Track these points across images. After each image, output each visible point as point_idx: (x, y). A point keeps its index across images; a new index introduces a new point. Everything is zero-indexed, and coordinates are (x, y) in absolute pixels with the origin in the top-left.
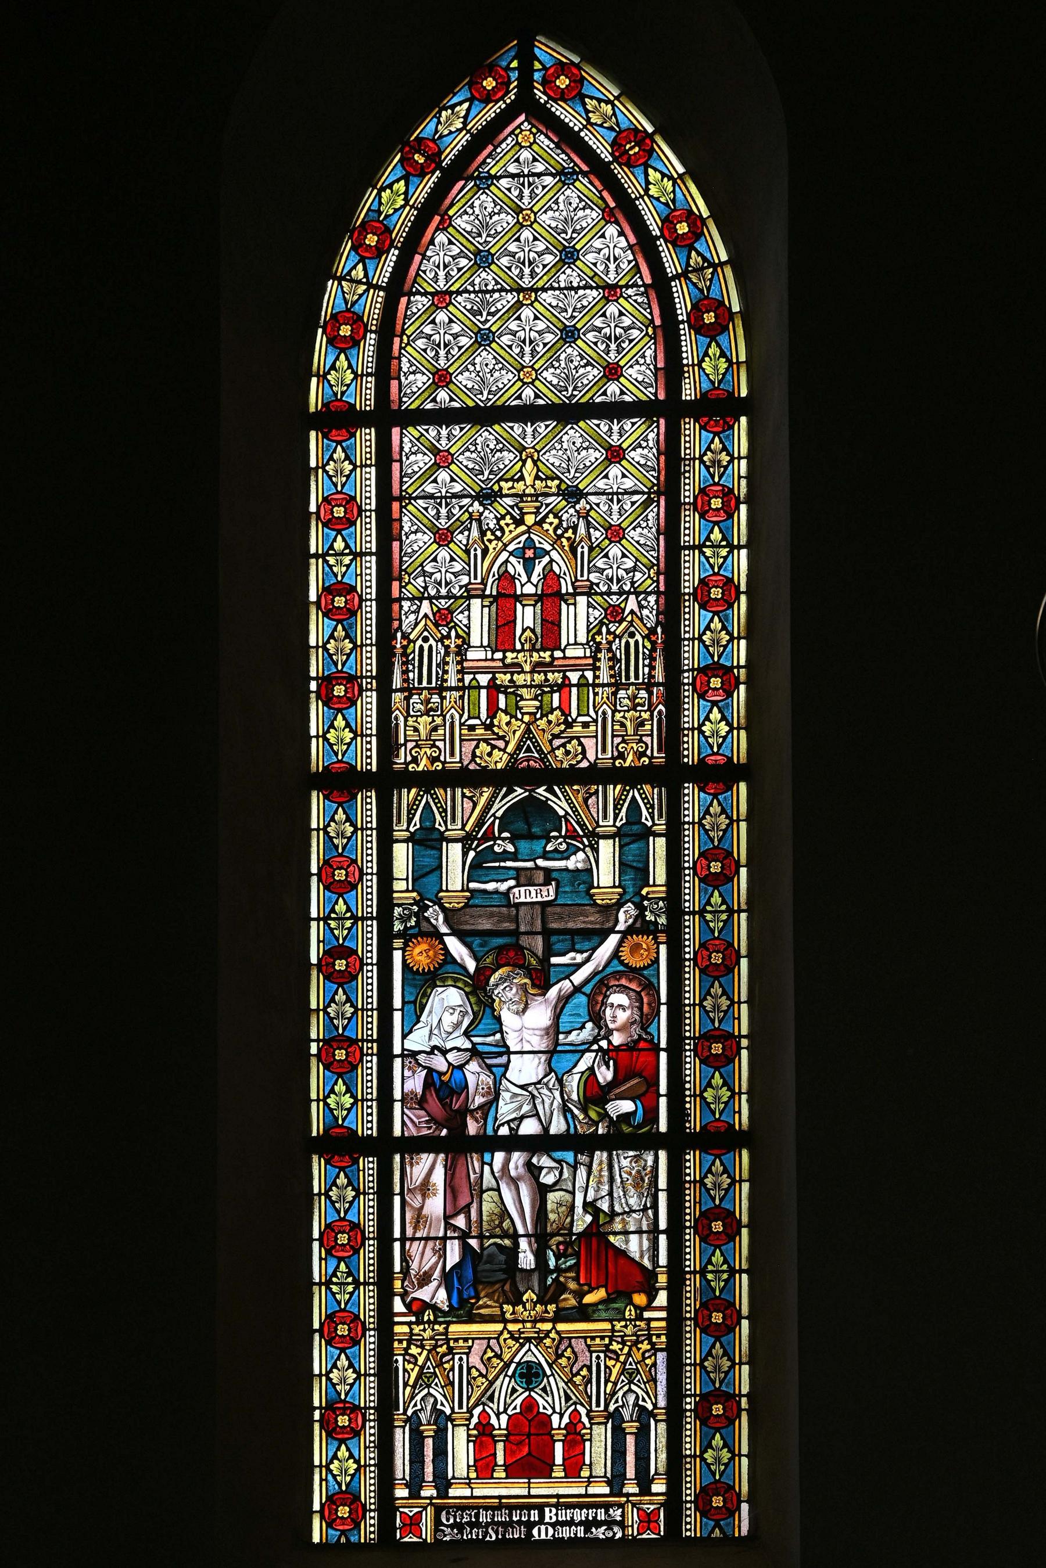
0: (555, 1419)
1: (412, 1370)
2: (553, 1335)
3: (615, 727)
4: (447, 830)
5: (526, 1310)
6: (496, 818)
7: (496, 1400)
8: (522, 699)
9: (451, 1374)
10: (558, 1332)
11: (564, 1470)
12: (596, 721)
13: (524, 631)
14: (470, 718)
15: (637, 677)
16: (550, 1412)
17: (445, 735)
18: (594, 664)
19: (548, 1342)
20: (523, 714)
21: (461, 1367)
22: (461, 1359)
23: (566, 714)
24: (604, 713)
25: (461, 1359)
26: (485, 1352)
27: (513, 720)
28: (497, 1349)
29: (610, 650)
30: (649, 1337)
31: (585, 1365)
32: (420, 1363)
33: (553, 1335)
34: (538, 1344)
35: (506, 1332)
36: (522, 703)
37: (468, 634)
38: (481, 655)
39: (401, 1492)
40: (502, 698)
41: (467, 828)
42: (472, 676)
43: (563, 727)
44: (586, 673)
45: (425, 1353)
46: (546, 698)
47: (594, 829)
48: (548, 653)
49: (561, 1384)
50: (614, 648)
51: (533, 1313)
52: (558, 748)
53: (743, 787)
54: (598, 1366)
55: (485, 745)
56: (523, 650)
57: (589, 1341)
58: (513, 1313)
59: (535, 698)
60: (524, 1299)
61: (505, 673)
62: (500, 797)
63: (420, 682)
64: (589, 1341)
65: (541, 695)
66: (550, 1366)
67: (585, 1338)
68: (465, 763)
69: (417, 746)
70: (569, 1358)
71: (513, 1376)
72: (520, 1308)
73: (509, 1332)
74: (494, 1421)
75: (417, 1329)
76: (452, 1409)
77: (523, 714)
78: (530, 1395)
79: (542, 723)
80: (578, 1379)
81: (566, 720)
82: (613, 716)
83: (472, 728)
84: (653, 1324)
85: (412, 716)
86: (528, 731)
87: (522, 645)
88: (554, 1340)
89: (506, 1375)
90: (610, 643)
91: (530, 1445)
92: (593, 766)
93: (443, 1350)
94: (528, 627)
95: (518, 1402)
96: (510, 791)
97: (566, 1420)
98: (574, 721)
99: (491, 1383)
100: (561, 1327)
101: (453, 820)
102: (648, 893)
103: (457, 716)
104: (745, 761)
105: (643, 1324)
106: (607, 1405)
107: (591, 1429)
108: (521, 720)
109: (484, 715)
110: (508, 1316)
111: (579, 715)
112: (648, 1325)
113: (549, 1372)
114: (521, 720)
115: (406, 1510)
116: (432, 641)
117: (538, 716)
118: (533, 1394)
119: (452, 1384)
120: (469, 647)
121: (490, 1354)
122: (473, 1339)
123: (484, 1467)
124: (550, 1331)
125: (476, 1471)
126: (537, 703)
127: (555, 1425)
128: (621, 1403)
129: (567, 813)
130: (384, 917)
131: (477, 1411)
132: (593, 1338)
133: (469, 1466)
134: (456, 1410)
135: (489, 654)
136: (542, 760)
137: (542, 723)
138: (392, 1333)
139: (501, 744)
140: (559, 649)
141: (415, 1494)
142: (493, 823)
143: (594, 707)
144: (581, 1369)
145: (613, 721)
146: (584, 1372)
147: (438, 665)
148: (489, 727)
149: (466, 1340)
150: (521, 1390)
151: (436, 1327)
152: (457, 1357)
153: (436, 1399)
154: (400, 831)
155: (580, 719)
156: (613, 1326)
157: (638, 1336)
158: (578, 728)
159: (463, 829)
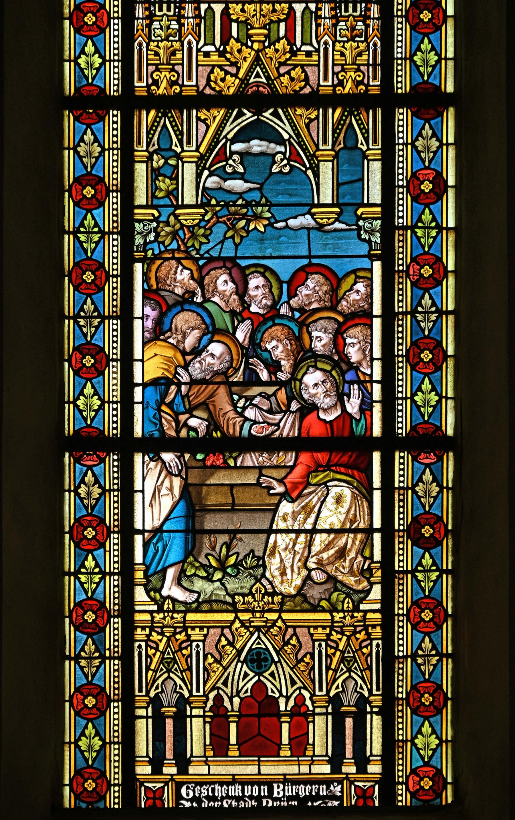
0: (282, 702)
1: (154, 655)
2: (280, 623)
3: (336, 57)
4: (183, 151)
5: (255, 601)
6: (227, 140)
7: (229, 685)
8: (253, 28)
9: (189, 659)
10: (283, 621)
11: (290, 749)
16: (277, 695)
17: (183, 59)
19: (274, 631)
20: (253, 42)
21: (198, 653)
22: (198, 646)
23: (291, 42)
25: (198, 646)
26: (219, 641)
27: (244, 47)
28: (230, 638)
30: (366, 628)
31: (308, 653)
32: (161, 648)
33: (280, 623)
34: (267, 632)
35: (237, 621)
36: (251, 32)
39: (143, 770)
40: (234, 26)
41: (202, 149)
42: (206, 5)
43: (288, 56)
44: (310, 5)
45: (165, 639)
46: (274, 26)
47: (314, 153)
49: (287, 670)
52: (283, 75)
53: (451, 110)
54: (320, 652)
55: (219, 70)
57: (312, 630)
58: (244, 603)
59: (264, 27)
62: (231, 119)
64: (312, 630)
65: (269, 24)
66: (278, 653)
67: (309, 627)
68: (201, 88)
69: (157, 70)
70: (294, 646)
71: (245, 661)
73: (241, 621)
74: (227, 703)
75: (158, 617)
76: (190, 692)
77: (253, 42)
78: (259, 680)
80: (302, 666)
81: (291, 48)
82: (334, 45)
83: (207, 54)
84: (369, 615)
85: (154, 41)
86: (257, 60)
88: (280, 628)
89: (239, 661)
91: (258, 725)
92: (315, 93)
93: (181, 637)
95: (249, 685)
96: (240, 114)
97: (291, 703)
98: (299, 50)
99: (225, 669)
100: (285, 616)
101: (189, 142)
104: (452, 91)
105: (358, 615)
106: (328, 691)
107: (314, 710)
108: (251, 48)
109: (218, 43)
110: (240, 606)
111: (303, 44)
112: (365, 616)
113: (276, 659)
114: (251, 48)
115: (150, 785)
117: (267, 44)
118: (262, 678)
119: (190, 669)
121: (224, 642)
122: (208, 628)
123: (219, 745)
124: (276, 621)
125: (212, 749)
126: (265, 31)
127: (282, 707)
128: (341, 689)
129: (291, 136)
130: (127, 231)
131: (212, 696)
132: (316, 628)
133: (205, 745)
134: (194, 693)
136: (268, 84)
137: (270, 52)
138: (133, 621)
139: (233, 70)
141: (157, 770)
142: (225, 144)
144: (305, 656)
145: (333, 50)
146: (307, 659)
148: (222, 54)
149: (201, 628)
150: (252, 674)
151: (175, 615)
152: (194, 644)
153: (175, 683)
154: (140, 151)
155: (304, 48)
156: (333, 617)
157: (355, 627)
158: (301, 57)
159: (197, 150)
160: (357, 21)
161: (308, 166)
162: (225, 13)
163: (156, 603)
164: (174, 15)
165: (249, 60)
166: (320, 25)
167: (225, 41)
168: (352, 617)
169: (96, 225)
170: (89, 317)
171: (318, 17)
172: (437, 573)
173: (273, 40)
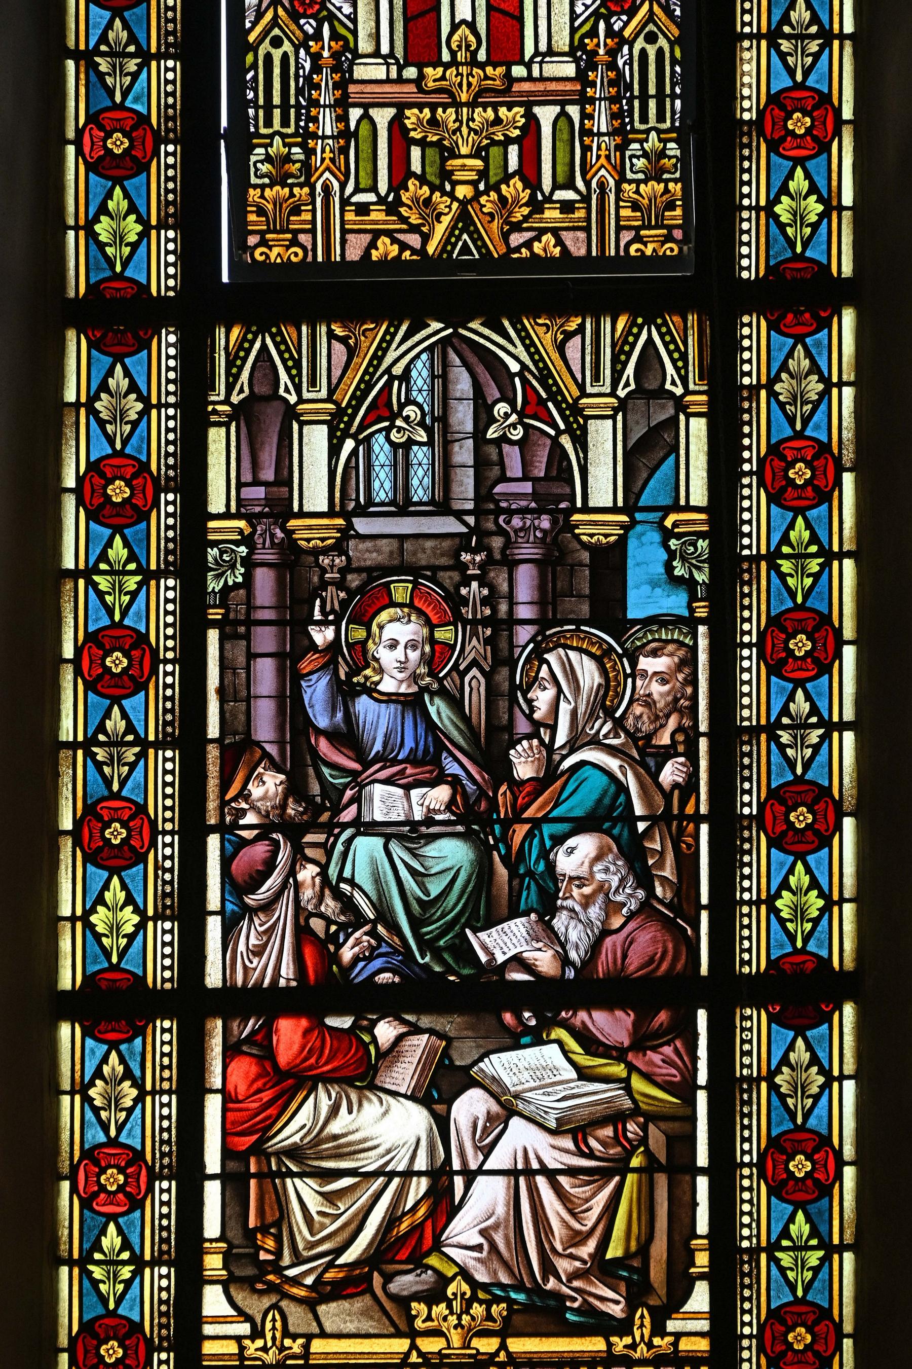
5: (452, 1313)
12: (586, 199)
13: (455, 27)
14: (357, 190)
15: (661, 118)
18: (583, 92)
20: (454, 184)
24: (602, 185)
29: (612, 65)
37: (355, 33)
38: (380, 72)
40: (416, 153)
43: (526, 211)
48: (500, 70)
50: (620, 63)
51: (466, 1319)
56: (454, 63)
58: (429, 1318)
60: (450, 1290)
61: (421, 107)
63: (268, 123)
65: (487, 148)
72: (440, 1309)
73: (420, 1354)
75: (252, 1347)
79: (488, 202)
81: (533, 196)
82: (619, 190)
83: (363, 209)
87: (453, 54)
90: (613, 53)
94: (463, 22)
98: (549, 199)
102: (675, 524)
103: (336, 185)
108: (452, 195)
109: (383, 187)
110: (419, 1324)
111: (556, 187)
112: (675, 1344)
114: (452, 195)
116: (287, 46)
117: (482, 187)
120: (356, 55)
124: (496, 1354)
135: (394, 69)
140: (521, 62)
143: (584, 173)
147: (299, 92)
148: (392, 208)
158: (552, 214)
160: (665, 141)
161: (562, 427)
162: (397, 125)
163: (249, 1318)
164: (296, 134)
165: (446, 220)
166: (590, 148)
167: (398, 182)
168: (650, 1345)
169: (130, 728)
170: (117, 743)
171: (586, 132)
172: (821, 1253)
173: (493, 180)
